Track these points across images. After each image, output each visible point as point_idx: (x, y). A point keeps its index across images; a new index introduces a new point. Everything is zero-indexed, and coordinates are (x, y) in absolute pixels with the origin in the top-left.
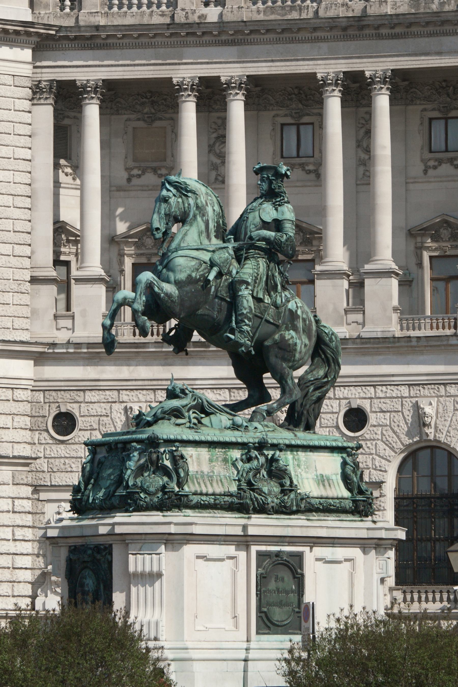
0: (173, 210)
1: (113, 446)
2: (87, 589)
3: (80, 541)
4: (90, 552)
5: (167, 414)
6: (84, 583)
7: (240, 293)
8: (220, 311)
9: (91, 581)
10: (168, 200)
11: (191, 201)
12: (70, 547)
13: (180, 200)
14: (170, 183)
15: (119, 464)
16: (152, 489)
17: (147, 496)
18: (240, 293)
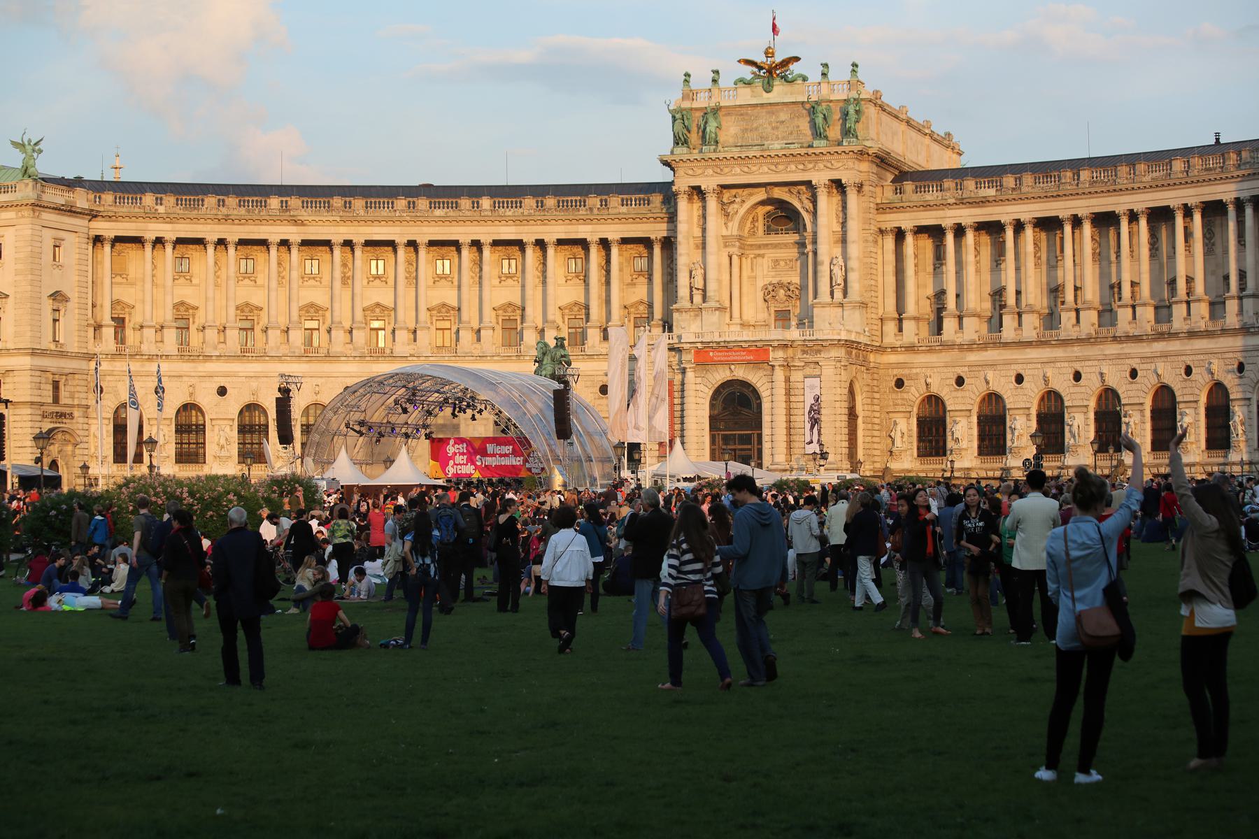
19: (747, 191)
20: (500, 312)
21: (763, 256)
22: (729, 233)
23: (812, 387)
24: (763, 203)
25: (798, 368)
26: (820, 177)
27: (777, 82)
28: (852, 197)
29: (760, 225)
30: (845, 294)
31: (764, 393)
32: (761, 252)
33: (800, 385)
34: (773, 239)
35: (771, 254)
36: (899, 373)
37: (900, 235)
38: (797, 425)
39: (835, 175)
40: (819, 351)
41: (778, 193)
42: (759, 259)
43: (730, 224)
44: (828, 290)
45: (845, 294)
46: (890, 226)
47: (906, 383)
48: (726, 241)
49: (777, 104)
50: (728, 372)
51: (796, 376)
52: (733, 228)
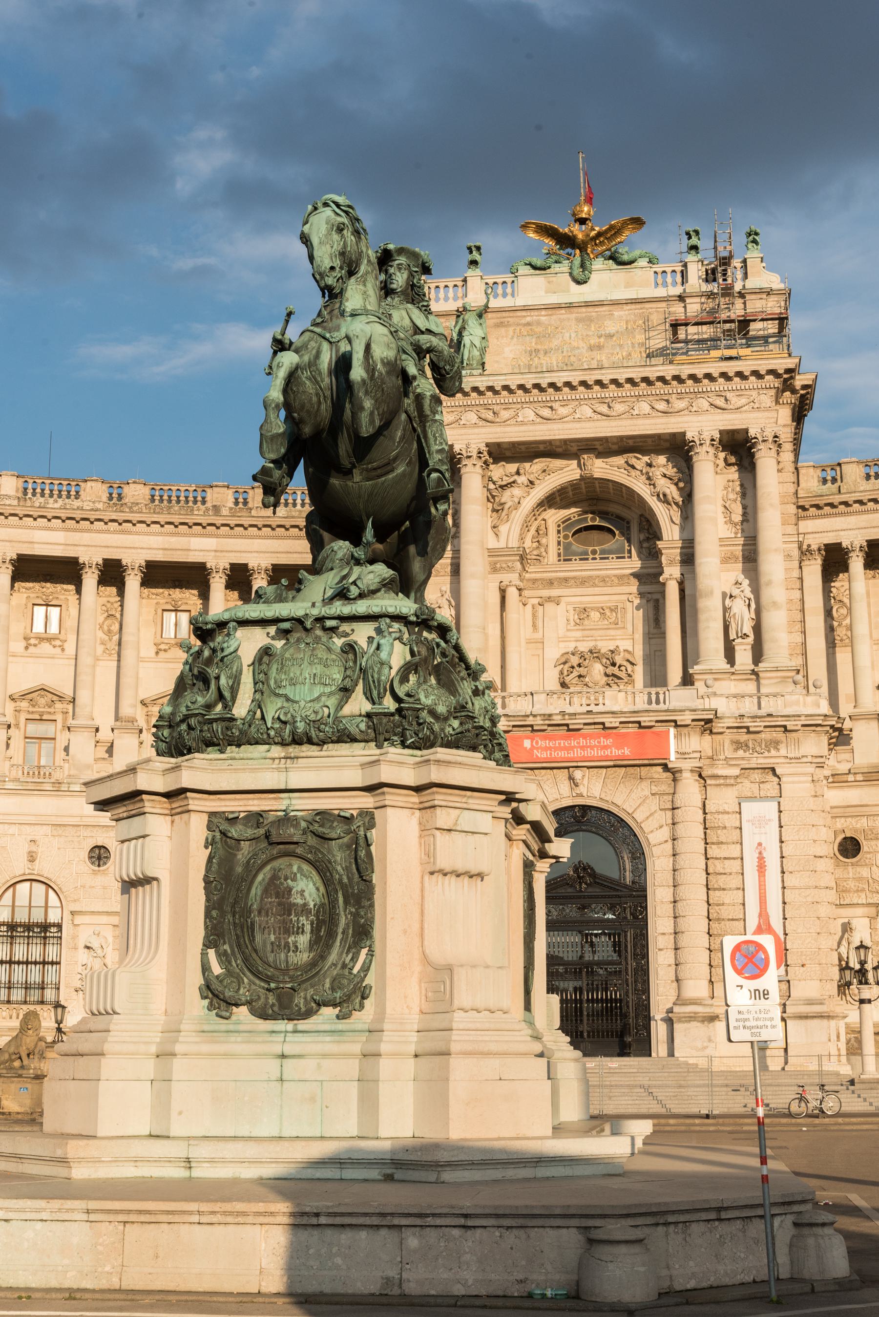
0: (349, 249)
1: (308, 624)
2: (299, 901)
3: (255, 804)
4: (303, 824)
5: (384, 586)
6: (290, 890)
7: (437, 417)
8: (403, 437)
9: (311, 885)
10: (342, 230)
11: (364, 250)
12: (212, 814)
13: (353, 238)
14: (338, 205)
15: (334, 657)
16: (441, 709)
17: (432, 720)
18: (437, 417)
19: (539, 464)
20: (24, 704)
21: (557, 601)
22: (502, 544)
23: (760, 822)
24: (551, 501)
25: (726, 782)
26: (702, 424)
27: (598, 264)
28: (766, 463)
29: (552, 540)
30: (758, 654)
31: (653, 833)
32: (554, 592)
33: (731, 821)
34: (576, 568)
35: (574, 597)
36: (852, 826)
37: (834, 560)
38: (725, 912)
39: (732, 421)
40: (776, 744)
41: (602, 468)
42: (550, 607)
43: (503, 529)
44: (719, 645)
45: (758, 654)
46: (815, 542)
47: (865, 846)
48: (496, 560)
49: (600, 304)
50: (565, 787)
51: (722, 799)
52: (511, 534)
